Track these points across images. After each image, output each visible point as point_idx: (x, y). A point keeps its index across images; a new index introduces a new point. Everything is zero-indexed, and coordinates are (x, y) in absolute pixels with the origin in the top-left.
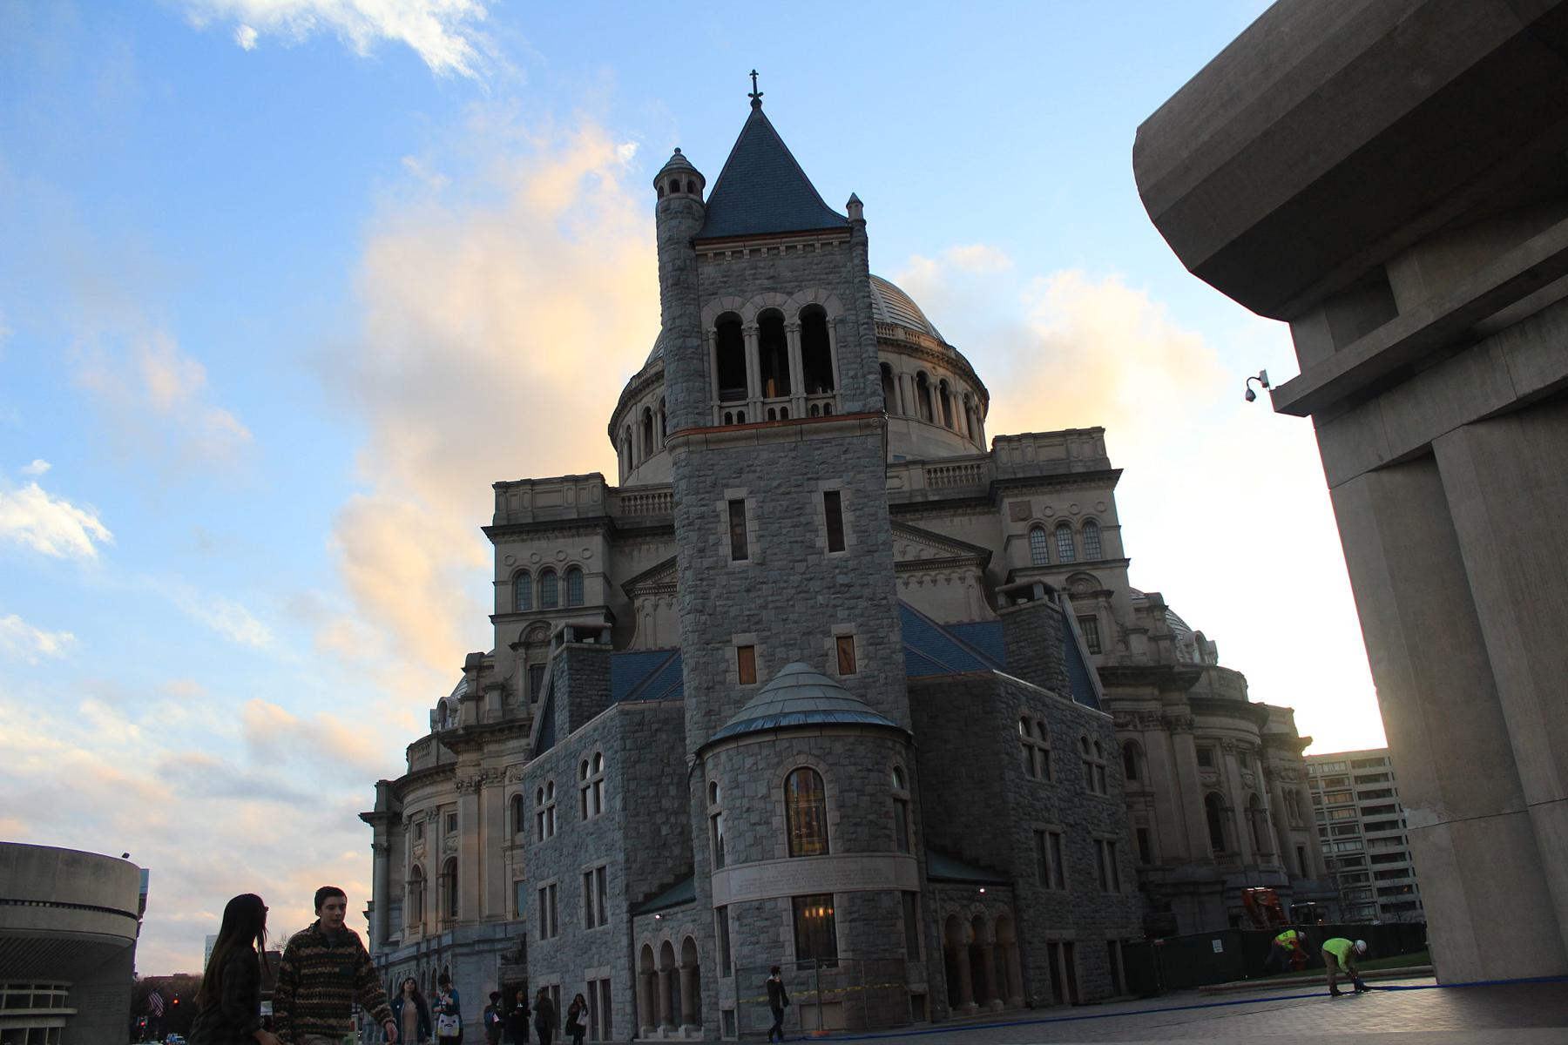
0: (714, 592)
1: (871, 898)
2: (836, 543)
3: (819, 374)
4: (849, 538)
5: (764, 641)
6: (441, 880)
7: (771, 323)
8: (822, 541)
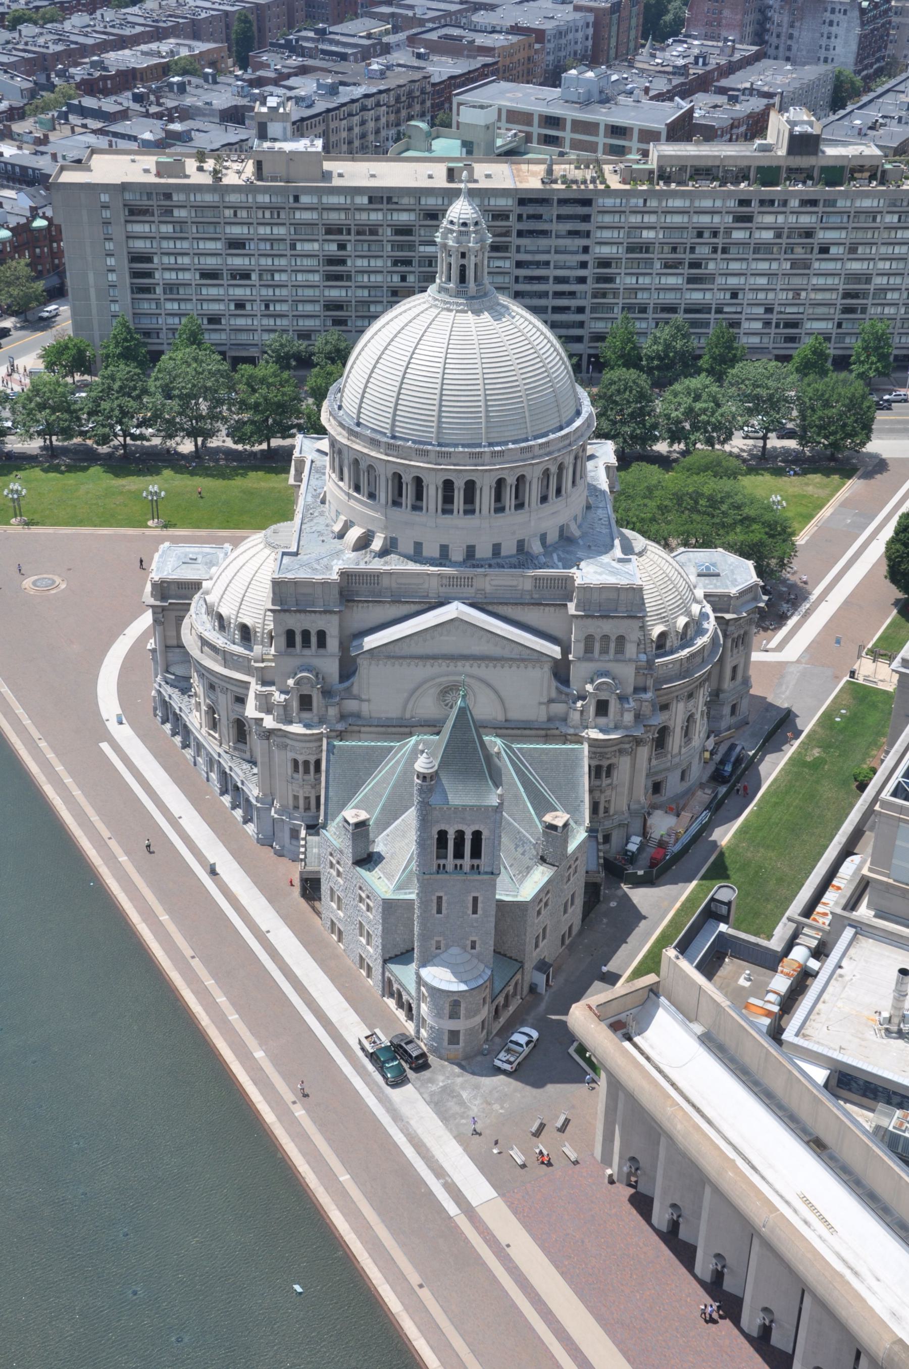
0: (429, 925)
1: (471, 1029)
2: (475, 911)
3: (476, 853)
4: (480, 911)
6: (231, 725)
7: (460, 835)
8: (470, 911)
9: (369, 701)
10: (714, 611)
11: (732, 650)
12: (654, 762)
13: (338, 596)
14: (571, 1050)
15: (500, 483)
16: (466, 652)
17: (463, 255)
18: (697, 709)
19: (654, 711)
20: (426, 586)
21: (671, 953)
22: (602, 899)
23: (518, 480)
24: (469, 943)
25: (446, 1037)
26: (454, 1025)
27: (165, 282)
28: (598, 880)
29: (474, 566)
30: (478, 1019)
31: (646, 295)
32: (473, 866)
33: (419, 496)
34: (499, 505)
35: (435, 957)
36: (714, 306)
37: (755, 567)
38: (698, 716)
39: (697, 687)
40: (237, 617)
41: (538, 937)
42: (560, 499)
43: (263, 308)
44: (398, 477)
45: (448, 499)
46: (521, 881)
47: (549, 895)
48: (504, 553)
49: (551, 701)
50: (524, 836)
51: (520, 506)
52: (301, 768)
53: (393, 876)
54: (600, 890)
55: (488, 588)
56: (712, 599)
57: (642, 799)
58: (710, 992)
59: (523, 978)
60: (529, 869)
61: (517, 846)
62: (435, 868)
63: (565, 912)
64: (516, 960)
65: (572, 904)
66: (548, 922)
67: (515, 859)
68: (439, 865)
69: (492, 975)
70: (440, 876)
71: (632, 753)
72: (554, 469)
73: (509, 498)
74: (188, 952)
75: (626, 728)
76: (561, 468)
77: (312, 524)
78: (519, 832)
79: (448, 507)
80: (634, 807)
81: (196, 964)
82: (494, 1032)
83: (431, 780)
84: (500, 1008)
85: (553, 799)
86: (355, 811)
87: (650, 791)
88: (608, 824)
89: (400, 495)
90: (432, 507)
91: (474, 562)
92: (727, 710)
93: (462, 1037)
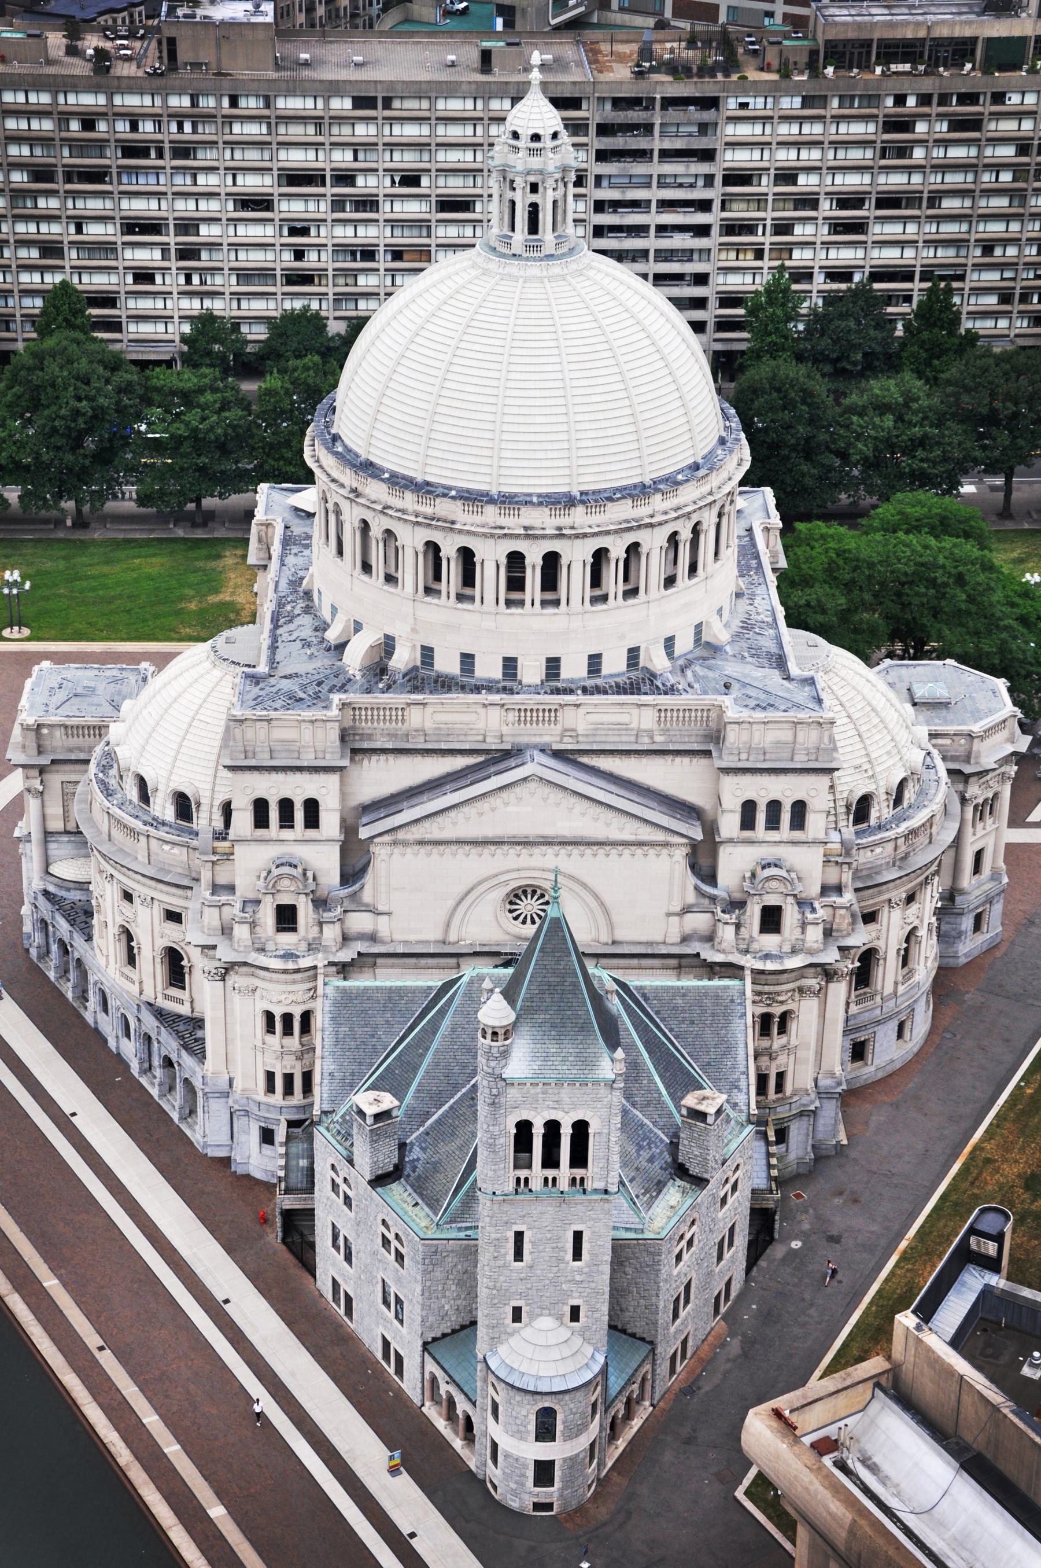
2: (577, 1255)
3: (579, 1159)
5: (527, 1305)
6: (158, 960)
7: (553, 1128)
8: (569, 1255)
9: (389, 914)
10: (944, 759)
11: (974, 826)
12: (854, 1009)
13: (338, 743)
14: (740, 1494)
15: (600, 556)
16: (550, 831)
17: (534, 188)
18: (922, 921)
19: (854, 923)
20: (481, 725)
21: (906, 1319)
22: (776, 1236)
23: (627, 551)
24: (567, 1310)
25: (530, 1473)
26: (544, 1451)
27: (17, 237)
28: (771, 1205)
29: (557, 691)
30: (583, 1442)
31: (808, 254)
32: (574, 1180)
33: (468, 578)
34: (598, 592)
35: (511, 1335)
36: (918, 269)
37: (1010, 690)
38: (922, 932)
39: (921, 884)
40: (169, 779)
41: (677, 1299)
42: (695, 580)
43: (182, 280)
44: (433, 549)
45: (516, 583)
46: (649, 1205)
47: (694, 1228)
48: (606, 670)
49: (686, 910)
50: (651, 1131)
51: (632, 593)
52: (278, 1026)
53: (437, 1201)
54: (774, 1221)
55: (581, 728)
56: (940, 741)
57: (838, 1070)
58: (978, 1387)
59: (654, 1370)
60: (660, 1186)
61: (640, 1148)
62: (511, 1186)
63: (720, 1258)
64: (643, 1339)
65: (731, 1244)
66: (694, 1276)
67: (637, 1169)
68: (518, 1180)
69: (606, 1364)
70: (518, 1197)
71: (821, 993)
72: (685, 535)
73: (612, 580)
74: (92, 1339)
75: (811, 952)
76: (696, 531)
77: (291, 627)
78: (642, 1125)
79: (515, 596)
80: (825, 1082)
81: (107, 1360)
82: (610, 1464)
83: (506, 1039)
84: (619, 1421)
85: (696, 1070)
86: (373, 1094)
87: (848, 1055)
88: (783, 1112)
89: (437, 577)
90: (490, 596)
91: (559, 685)
92: (967, 923)
93: (558, 1473)
